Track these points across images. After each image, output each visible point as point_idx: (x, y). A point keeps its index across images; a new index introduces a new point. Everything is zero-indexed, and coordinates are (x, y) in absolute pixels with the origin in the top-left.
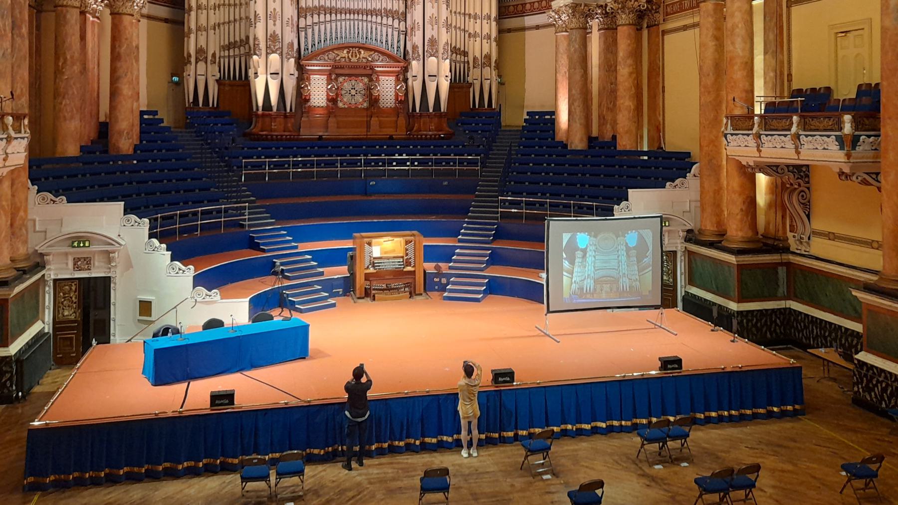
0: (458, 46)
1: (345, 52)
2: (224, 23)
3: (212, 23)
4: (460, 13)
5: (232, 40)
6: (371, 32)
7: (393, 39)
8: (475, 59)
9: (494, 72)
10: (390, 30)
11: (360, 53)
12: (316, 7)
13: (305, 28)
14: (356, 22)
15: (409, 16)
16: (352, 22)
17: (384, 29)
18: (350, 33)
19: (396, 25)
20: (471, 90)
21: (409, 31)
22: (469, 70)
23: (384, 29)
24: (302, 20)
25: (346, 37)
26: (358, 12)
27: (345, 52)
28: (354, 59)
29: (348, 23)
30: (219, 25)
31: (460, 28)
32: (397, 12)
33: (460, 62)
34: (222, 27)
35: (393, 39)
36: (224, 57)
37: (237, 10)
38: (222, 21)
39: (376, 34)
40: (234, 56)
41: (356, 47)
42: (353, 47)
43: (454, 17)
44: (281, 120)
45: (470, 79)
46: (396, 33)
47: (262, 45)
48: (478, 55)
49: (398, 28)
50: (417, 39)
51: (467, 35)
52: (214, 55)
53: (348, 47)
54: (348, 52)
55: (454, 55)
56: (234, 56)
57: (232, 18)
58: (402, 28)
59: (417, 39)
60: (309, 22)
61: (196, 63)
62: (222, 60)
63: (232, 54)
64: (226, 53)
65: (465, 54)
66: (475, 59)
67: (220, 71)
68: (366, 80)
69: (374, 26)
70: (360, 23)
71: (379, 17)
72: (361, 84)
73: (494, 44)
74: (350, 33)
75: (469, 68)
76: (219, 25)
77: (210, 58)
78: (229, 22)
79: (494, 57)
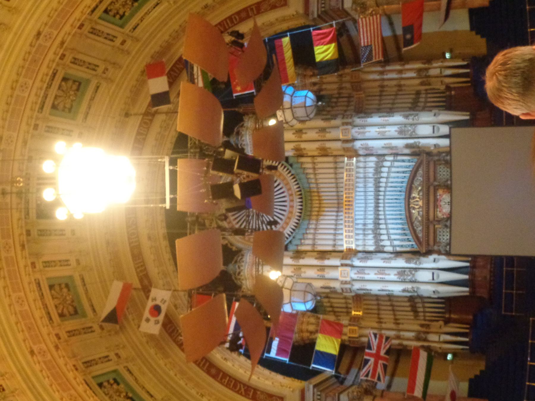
0: (410, 100)
1: (414, 211)
2: (395, 315)
3: (393, 326)
4: (380, 100)
5: (409, 309)
6: (395, 187)
7: (401, 167)
8: (422, 84)
9: (435, 65)
10: (393, 170)
11: (414, 198)
12: (374, 237)
13: (394, 246)
14: (386, 201)
15: (380, 152)
16: (387, 205)
17: (392, 175)
18: (396, 207)
19: (388, 164)
20: (452, 86)
21: (394, 151)
22: (434, 89)
23: (392, 175)
24: (386, 249)
25: (400, 210)
26: (377, 199)
27: (414, 211)
28: (420, 203)
29: (387, 209)
30: (396, 319)
31: (394, 100)
32: (377, 163)
33: (426, 98)
34: (398, 317)
35: (401, 167)
36: (424, 316)
37: (382, 303)
38: (392, 317)
39: (397, 182)
40: (424, 307)
41: (409, 202)
42: (409, 205)
43: (383, 106)
44: (477, 272)
45: (443, 88)
46: (396, 164)
47: (409, 286)
48: (417, 81)
49: (392, 161)
50: (400, 143)
51: (400, 93)
52: (422, 326)
53: (409, 208)
54: (414, 209)
55: (419, 104)
56: (424, 307)
57: (390, 308)
58: (391, 158)
59: (400, 143)
60: (388, 243)
61: (428, 341)
62: (427, 318)
63: (421, 310)
64: (422, 314)
65: (418, 93)
66: (422, 84)
67: (437, 321)
68: (440, 192)
69: (390, 185)
70: (387, 197)
71: (382, 180)
72: (444, 196)
73: (407, 67)
74: (396, 207)
75: (431, 89)
76: (396, 319)
77: (424, 329)
78: (393, 310)
79: (418, 65)
